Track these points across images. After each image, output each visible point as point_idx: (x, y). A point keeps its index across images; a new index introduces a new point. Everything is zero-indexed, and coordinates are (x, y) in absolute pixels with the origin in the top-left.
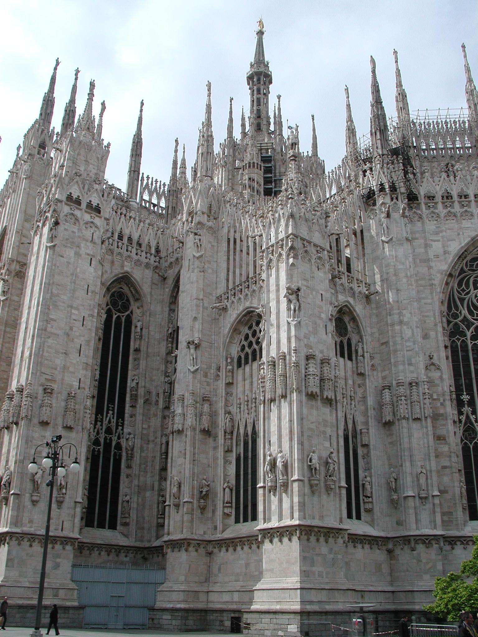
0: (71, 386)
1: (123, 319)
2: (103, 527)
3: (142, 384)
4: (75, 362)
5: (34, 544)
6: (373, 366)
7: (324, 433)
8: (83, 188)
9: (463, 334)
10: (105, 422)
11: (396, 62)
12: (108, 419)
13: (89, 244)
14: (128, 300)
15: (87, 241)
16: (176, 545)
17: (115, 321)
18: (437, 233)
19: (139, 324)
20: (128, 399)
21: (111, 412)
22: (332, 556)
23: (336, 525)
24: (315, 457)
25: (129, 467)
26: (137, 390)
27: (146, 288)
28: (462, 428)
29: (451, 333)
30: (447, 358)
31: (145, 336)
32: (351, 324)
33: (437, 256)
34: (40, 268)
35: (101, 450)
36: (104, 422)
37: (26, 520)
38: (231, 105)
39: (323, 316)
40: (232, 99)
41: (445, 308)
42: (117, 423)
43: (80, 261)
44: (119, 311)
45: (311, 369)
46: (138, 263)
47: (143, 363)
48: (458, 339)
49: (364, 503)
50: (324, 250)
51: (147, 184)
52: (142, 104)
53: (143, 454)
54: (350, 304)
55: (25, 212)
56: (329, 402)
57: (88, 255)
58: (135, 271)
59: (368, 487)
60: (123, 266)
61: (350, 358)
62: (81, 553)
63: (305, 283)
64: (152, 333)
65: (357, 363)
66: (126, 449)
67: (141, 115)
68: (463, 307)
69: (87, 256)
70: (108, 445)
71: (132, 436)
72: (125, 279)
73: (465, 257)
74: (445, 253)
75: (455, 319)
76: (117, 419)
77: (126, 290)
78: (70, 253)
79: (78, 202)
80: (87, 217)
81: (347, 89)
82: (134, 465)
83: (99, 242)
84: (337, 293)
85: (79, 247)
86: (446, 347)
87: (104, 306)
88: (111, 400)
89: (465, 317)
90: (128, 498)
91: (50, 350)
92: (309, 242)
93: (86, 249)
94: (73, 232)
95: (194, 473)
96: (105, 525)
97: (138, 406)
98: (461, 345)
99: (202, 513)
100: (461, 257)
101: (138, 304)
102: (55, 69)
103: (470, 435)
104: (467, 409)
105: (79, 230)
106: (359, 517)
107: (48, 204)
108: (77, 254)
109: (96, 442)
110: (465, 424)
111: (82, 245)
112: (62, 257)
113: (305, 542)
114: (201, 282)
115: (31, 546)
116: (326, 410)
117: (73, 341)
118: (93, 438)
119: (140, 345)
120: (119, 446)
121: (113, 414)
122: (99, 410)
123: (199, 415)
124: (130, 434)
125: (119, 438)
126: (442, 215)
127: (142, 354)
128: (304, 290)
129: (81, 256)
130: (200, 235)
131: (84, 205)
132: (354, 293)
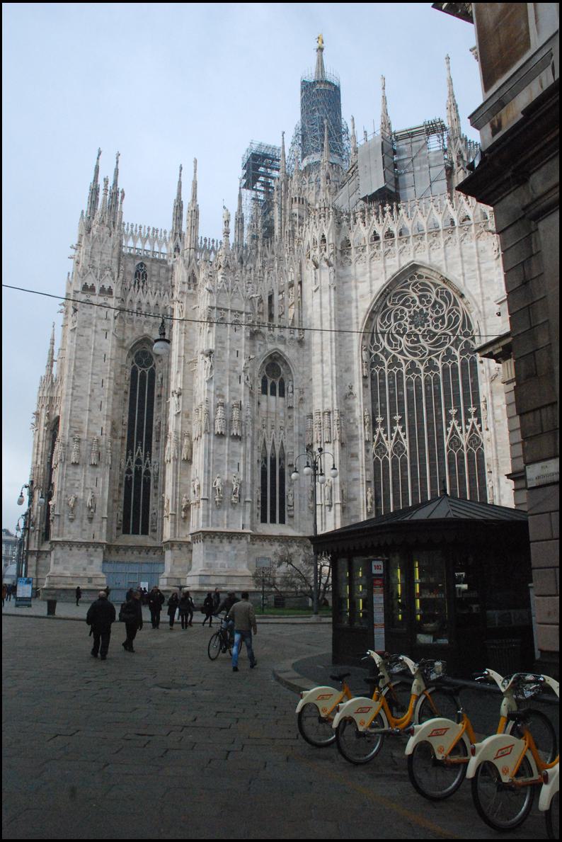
0: (95, 434)
1: (147, 373)
2: (138, 534)
4: (97, 415)
5: (73, 548)
6: (301, 399)
7: (233, 461)
9: (382, 364)
10: (136, 455)
11: (384, 88)
13: (104, 321)
16: (171, 544)
17: (140, 376)
18: (364, 275)
19: (160, 375)
20: (154, 436)
21: (139, 447)
22: (235, 552)
23: (240, 530)
24: (218, 481)
25: (156, 488)
26: (160, 428)
28: (374, 446)
29: (372, 363)
30: (365, 386)
32: (284, 366)
33: (362, 296)
35: (133, 477)
37: (66, 531)
38: (283, 139)
39: (237, 369)
40: (284, 133)
41: (367, 342)
44: (144, 367)
45: (219, 414)
48: (377, 369)
49: (288, 511)
50: (242, 313)
52: (181, 169)
54: (279, 350)
56: (237, 438)
58: (153, 333)
59: (290, 498)
61: (282, 395)
62: (118, 553)
63: (220, 345)
65: (288, 399)
67: (180, 179)
68: (384, 338)
70: (138, 472)
71: (157, 464)
73: (388, 294)
74: (371, 292)
75: (377, 351)
76: (146, 451)
79: (92, 289)
80: (101, 300)
81: (353, 119)
82: (159, 487)
83: (112, 318)
84: (266, 343)
86: (365, 377)
87: (131, 367)
88: (140, 438)
89: (385, 348)
90: (155, 511)
92: (227, 310)
94: (91, 315)
95: (176, 493)
96: (139, 531)
98: (379, 374)
99: (185, 522)
100: (385, 294)
103: (381, 450)
104: (380, 430)
106: (282, 521)
109: (129, 471)
110: (378, 441)
112: (82, 336)
113: (209, 543)
114: (183, 342)
115: (71, 550)
116: (236, 444)
117: (94, 399)
119: (161, 392)
120: (147, 473)
121: (142, 449)
122: (130, 446)
123: (179, 448)
124: (155, 462)
125: (147, 466)
126: (368, 257)
128: (219, 352)
130: (182, 303)
131: (97, 291)
132: (285, 341)
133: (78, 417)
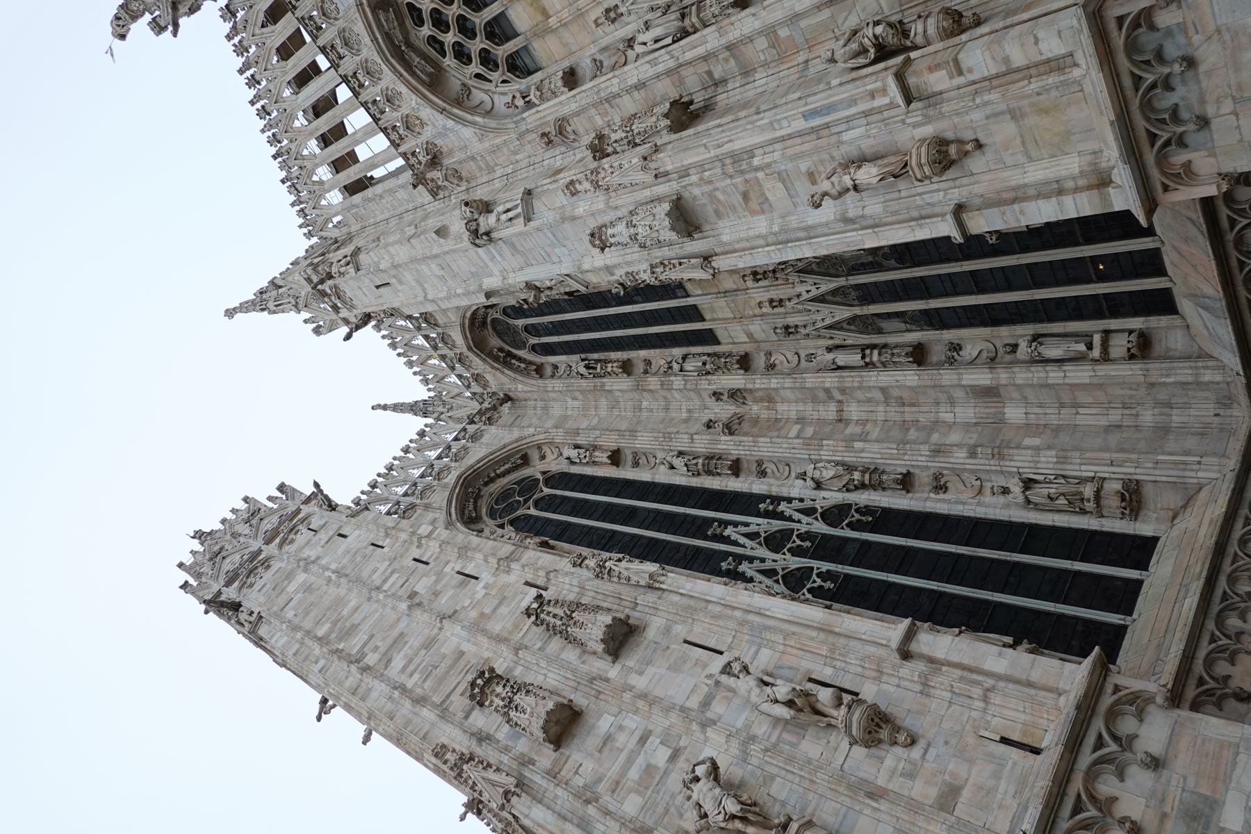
1: (547, 491)
3: (682, 443)
12: (742, 540)
21: (729, 531)
25: (906, 482)
35: (825, 566)
36: (749, 552)
42: (767, 515)
53: (875, 433)
66: (847, 488)
76: (759, 515)
88: (698, 528)
97: (735, 452)
118: (781, 588)
120: (834, 515)
125: (809, 512)
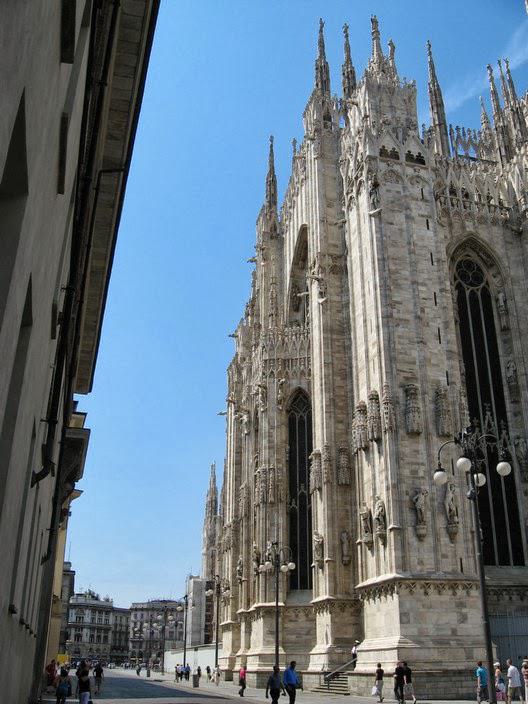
1: (479, 294)
4: (436, 351)
8: (397, 137)
10: (484, 427)
12: (486, 422)
13: (420, 203)
14: (479, 269)
15: (417, 200)
17: (470, 298)
20: (506, 393)
21: (488, 413)
26: (516, 380)
27: (499, 250)
31: (513, 311)
34: (367, 245)
42: (499, 426)
43: (414, 226)
44: (471, 284)
46: (482, 220)
47: (517, 345)
51: (458, 137)
55: (325, 196)
57: (422, 216)
58: (480, 231)
60: (463, 227)
64: (520, 305)
66: (518, 457)
69: (421, 218)
72: (471, 243)
76: (499, 422)
77: (474, 257)
78: (400, 218)
79: (395, 155)
80: (410, 171)
85: (408, 208)
91: (402, 340)
93: (418, 209)
94: (398, 192)
96: (509, 561)
101: (492, 272)
102: (321, 31)
105: (404, 188)
107: (359, 168)
108: (408, 217)
111: (412, 206)
112: (392, 224)
117: (428, 325)
121: (492, 415)
125: (505, 445)
127: (514, 334)
129: (413, 219)
131: (403, 158)
133: (406, 354)
